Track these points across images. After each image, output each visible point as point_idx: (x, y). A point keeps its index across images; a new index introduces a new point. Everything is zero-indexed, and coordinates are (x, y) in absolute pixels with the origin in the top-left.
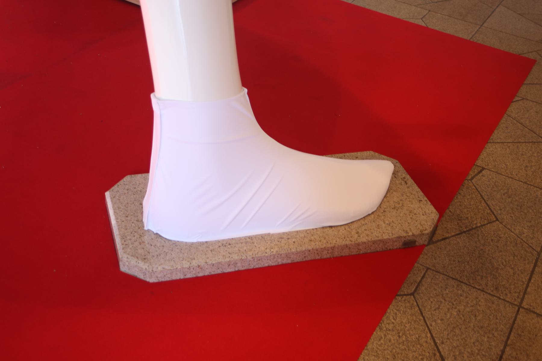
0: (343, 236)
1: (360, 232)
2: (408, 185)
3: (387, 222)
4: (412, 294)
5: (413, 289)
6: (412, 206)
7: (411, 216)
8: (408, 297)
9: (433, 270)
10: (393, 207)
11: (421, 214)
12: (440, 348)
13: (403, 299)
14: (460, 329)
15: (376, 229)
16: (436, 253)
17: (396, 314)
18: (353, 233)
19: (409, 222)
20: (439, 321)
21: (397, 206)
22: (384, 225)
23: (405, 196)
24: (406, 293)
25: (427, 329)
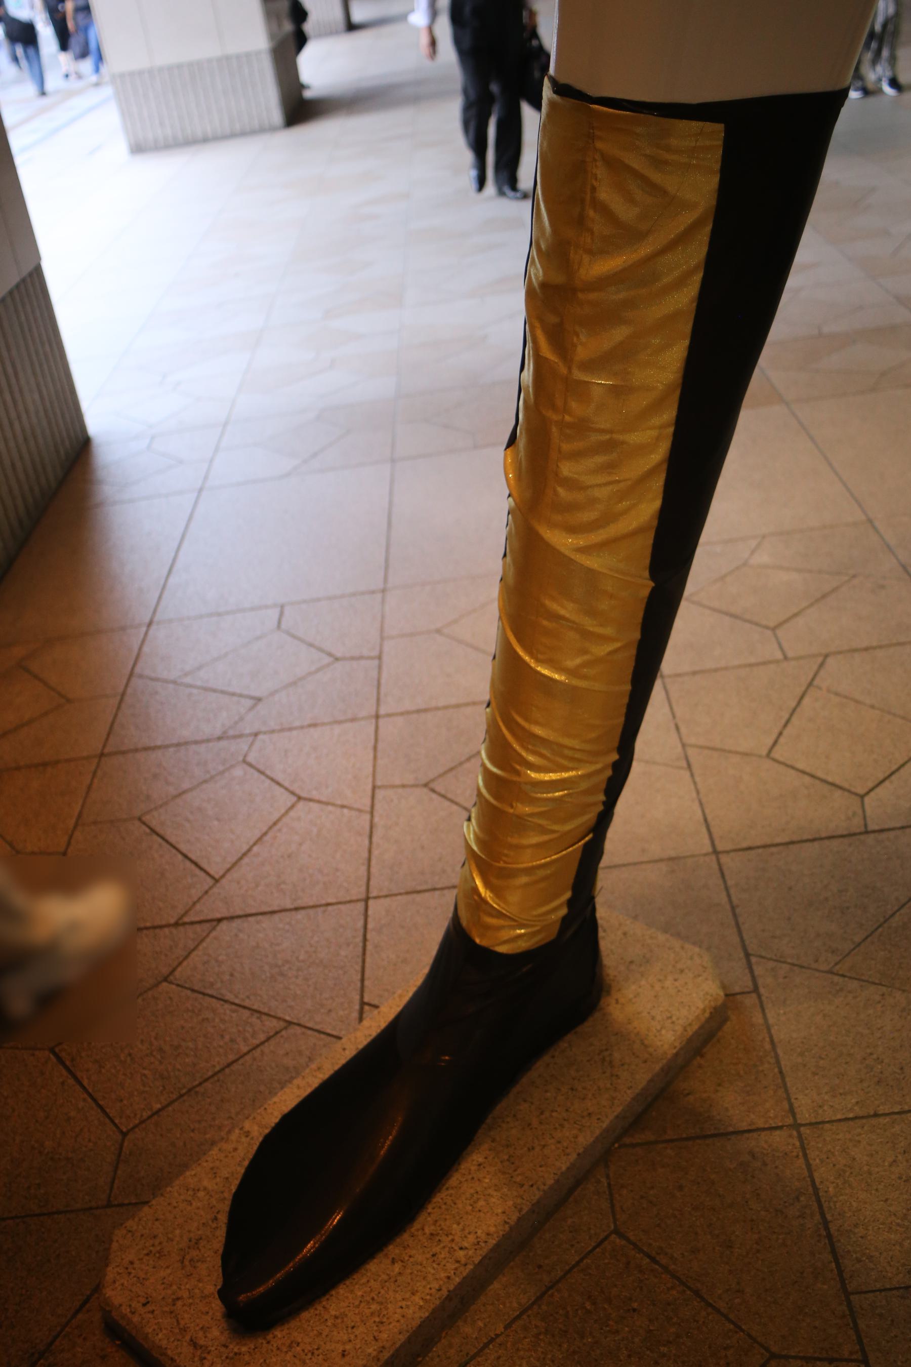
0: (269, 1111)
1: (243, 1139)
2: (188, 1338)
3: (201, 1194)
4: (124, 1135)
5: (126, 1144)
6: (162, 1274)
7: (157, 1242)
8: (131, 1125)
9: (97, 1208)
10: (202, 1243)
11: (137, 1264)
12: (64, 1072)
13: (138, 1116)
14: (37, 1121)
15: (217, 1163)
16: (97, 1252)
17: (144, 1086)
18: (256, 1128)
19: (157, 1223)
20: (73, 1114)
21: (194, 1253)
22: (205, 1183)
23: (185, 1295)
24: (137, 1130)
25: (90, 1091)
